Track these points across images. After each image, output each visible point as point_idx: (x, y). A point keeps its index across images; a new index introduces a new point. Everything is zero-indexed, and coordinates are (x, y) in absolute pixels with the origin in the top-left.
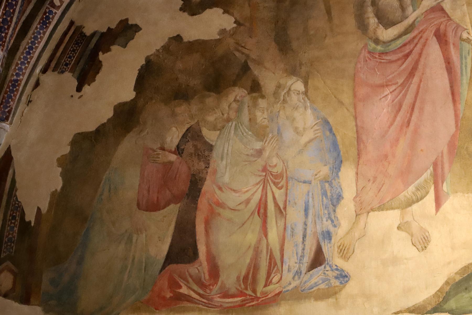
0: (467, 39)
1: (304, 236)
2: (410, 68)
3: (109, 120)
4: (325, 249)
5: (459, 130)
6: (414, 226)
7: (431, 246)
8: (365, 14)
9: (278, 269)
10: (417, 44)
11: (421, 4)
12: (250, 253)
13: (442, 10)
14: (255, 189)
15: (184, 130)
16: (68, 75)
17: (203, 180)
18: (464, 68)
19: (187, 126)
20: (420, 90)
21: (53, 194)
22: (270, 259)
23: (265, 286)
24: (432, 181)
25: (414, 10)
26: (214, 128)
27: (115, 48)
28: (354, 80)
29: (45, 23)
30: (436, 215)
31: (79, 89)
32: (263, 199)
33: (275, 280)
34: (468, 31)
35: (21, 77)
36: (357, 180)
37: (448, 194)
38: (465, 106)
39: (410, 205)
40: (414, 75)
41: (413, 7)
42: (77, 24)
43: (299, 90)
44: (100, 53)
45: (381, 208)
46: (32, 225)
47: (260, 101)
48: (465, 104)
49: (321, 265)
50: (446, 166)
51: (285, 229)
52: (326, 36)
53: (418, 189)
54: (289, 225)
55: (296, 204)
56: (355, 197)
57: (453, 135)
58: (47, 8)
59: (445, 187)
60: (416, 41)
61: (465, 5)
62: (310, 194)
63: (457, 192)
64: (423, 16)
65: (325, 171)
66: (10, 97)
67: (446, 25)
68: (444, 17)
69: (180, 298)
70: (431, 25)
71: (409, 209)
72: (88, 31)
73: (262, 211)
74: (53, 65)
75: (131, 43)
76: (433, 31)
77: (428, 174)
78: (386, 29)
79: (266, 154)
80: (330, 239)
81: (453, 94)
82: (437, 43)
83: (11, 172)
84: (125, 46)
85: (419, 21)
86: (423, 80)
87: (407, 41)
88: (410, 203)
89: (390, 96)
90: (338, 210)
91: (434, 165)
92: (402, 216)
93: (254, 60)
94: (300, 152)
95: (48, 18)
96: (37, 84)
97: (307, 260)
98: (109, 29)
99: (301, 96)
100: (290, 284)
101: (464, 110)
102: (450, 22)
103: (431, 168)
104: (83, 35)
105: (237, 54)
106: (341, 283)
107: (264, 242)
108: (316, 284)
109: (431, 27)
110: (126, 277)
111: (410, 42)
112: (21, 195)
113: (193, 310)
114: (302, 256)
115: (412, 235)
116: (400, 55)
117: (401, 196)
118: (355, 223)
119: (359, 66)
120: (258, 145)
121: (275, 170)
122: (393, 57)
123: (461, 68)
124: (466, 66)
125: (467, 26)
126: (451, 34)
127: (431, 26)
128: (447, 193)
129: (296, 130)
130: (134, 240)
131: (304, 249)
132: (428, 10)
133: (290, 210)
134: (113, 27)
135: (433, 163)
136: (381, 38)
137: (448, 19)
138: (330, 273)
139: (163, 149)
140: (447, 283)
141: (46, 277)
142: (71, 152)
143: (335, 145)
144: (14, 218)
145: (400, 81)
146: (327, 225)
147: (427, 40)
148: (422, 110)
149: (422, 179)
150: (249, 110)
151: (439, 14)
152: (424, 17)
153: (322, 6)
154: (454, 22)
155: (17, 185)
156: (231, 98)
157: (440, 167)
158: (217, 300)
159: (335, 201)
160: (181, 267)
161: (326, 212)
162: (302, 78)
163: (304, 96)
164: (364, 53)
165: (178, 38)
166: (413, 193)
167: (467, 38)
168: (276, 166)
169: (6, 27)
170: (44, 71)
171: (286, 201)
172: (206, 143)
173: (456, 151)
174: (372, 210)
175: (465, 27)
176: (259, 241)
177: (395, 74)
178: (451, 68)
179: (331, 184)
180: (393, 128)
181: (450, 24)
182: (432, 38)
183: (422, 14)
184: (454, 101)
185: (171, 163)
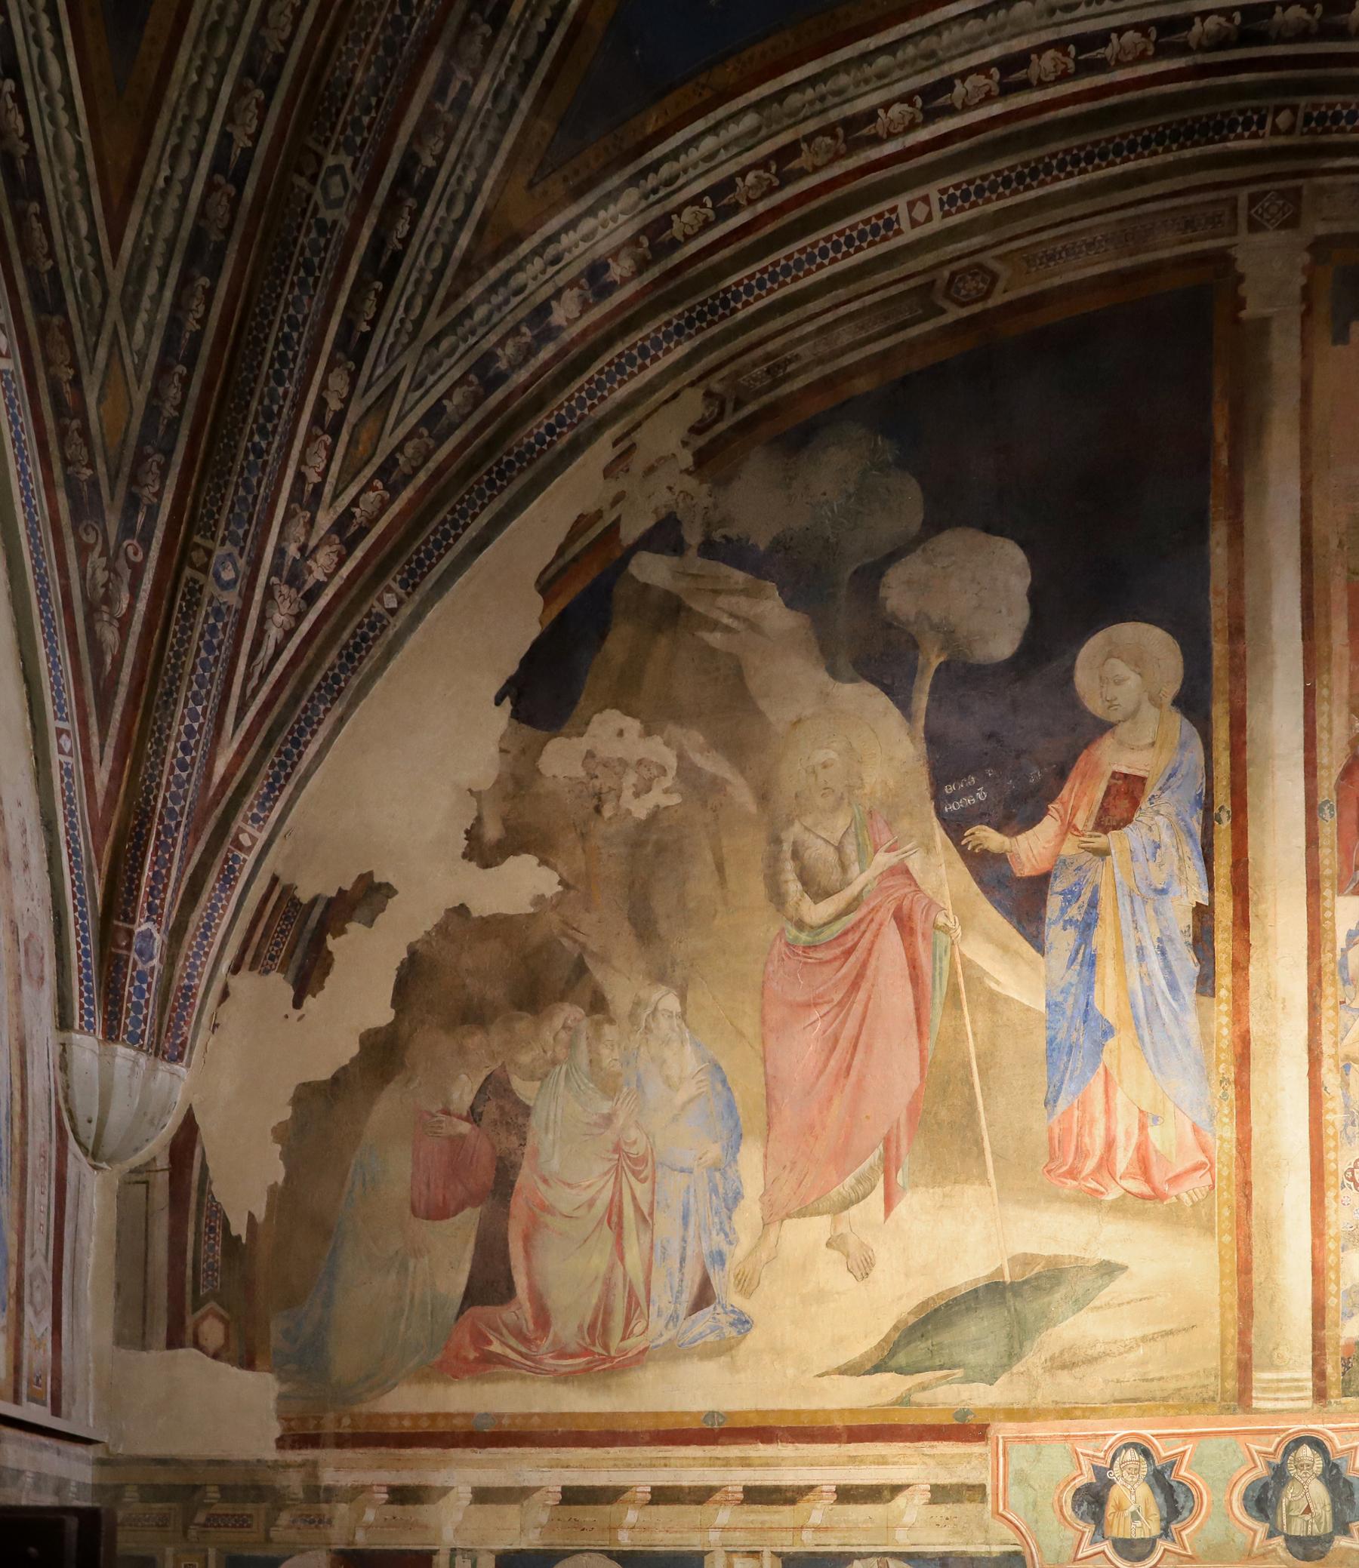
1: (683, 1260)
2: (854, 973)
3: (353, 1060)
4: (715, 1281)
6: (852, 1240)
7: (876, 1273)
9: (642, 1312)
12: (599, 1287)
13: (907, 872)
14: (602, 1183)
15: (481, 1080)
16: (276, 977)
17: (516, 1167)
19: (486, 1073)
21: (272, 1190)
22: (630, 1296)
23: (623, 1339)
25: (862, 871)
26: (532, 1078)
27: (353, 927)
28: (762, 994)
29: (228, 879)
31: (297, 1003)
32: (617, 1198)
33: (638, 1329)
35: (197, 981)
36: (765, 1168)
37: (904, 1189)
39: (847, 1208)
42: (284, 881)
44: (329, 937)
45: (802, 1213)
46: (244, 1241)
49: (708, 1305)
50: (904, 1142)
51: (652, 1248)
52: (716, 911)
53: (859, 1181)
54: (658, 1243)
55: (668, 1206)
56: (763, 1195)
58: (229, 850)
59: (900, 1178)
60: (863, 927)
62: (692, 1190)
65: (714, 1151)
66: (182, 1018)
69: (489, 1359)
71: (845, 1213)
72: (304, 895)
73: (614, 1219)
74: (249, 957)
75: (381, 918)
77: (874, 1158)
78: (816, 903)
79: (619, 1122)
80: (723, 1264)
83: (198, 1151)
84: (370, 923)
87: (849, 926)
88: (847, 1204)
89: (819, 1024)
90: (735, 1217)
92: (835, 1225)
93: (593, 955)
94: (675, 1119)
95: (231, 869)
96: (225, 994)
97: (688, 1297)
98: (341, 891)
99: (676, 1022)
100: (661, 1335)
103: (881, 1147)
104: (295, 903)
105: (566, 942)
106: (739, 1332)
107: (619, 1270)
108: (701, 1336)
110: (402, 1327)
111: (853, 928)
112: (221, 1190)
113: (512, 1378)
114: (680, 1292)
115: (848, 1256)
116: (838, 951)
117: (833, 1193)
118: (763, 1236)
119: (771, 968)
120: (606, 1107)
121: (633, 1150)
123: (934, 976)
129: (667, 1080)
130: (411, 1269)
131: (682, 1280)
133: (660, 1218)
134: (348, 887)
136: (807, 919)
138: (723, 1318)
139: (447, 1112)
140: (895, 1328)
141: (276, 1328)
142: (295, 1117)
143: (731, 1106)
144: (212, 1229)
145: (837, 997)
146: (718, 1241)
147: (881, 925)
148: (869, 1048)
149: (865, 1165)
150: (589, 1045)
151: (900, 880)
153: (709, 857)
155: (211, 1174)
156: (558, 1022)
157: (893, 1145)
158: (549, 1361)
159: (730, 1202)
160: (489, 1310)
161: (716, 1220)
162: (675, 987)
163: (680, 1021)
164: (780, 946)
165: (462, 910)
166: (852, 1188)
168: (635, 1142)
169: (161, 887)
170: (235, 969)
171: (652, 1203)
172: (518, 1102)
174: (789, 1216)
176: (612, 1268)
177: (830, 984)
178: (917, 976)
179: (724, 1174)
180: (823, 1079)
184: (920, 1034)
185: (462, 1137)
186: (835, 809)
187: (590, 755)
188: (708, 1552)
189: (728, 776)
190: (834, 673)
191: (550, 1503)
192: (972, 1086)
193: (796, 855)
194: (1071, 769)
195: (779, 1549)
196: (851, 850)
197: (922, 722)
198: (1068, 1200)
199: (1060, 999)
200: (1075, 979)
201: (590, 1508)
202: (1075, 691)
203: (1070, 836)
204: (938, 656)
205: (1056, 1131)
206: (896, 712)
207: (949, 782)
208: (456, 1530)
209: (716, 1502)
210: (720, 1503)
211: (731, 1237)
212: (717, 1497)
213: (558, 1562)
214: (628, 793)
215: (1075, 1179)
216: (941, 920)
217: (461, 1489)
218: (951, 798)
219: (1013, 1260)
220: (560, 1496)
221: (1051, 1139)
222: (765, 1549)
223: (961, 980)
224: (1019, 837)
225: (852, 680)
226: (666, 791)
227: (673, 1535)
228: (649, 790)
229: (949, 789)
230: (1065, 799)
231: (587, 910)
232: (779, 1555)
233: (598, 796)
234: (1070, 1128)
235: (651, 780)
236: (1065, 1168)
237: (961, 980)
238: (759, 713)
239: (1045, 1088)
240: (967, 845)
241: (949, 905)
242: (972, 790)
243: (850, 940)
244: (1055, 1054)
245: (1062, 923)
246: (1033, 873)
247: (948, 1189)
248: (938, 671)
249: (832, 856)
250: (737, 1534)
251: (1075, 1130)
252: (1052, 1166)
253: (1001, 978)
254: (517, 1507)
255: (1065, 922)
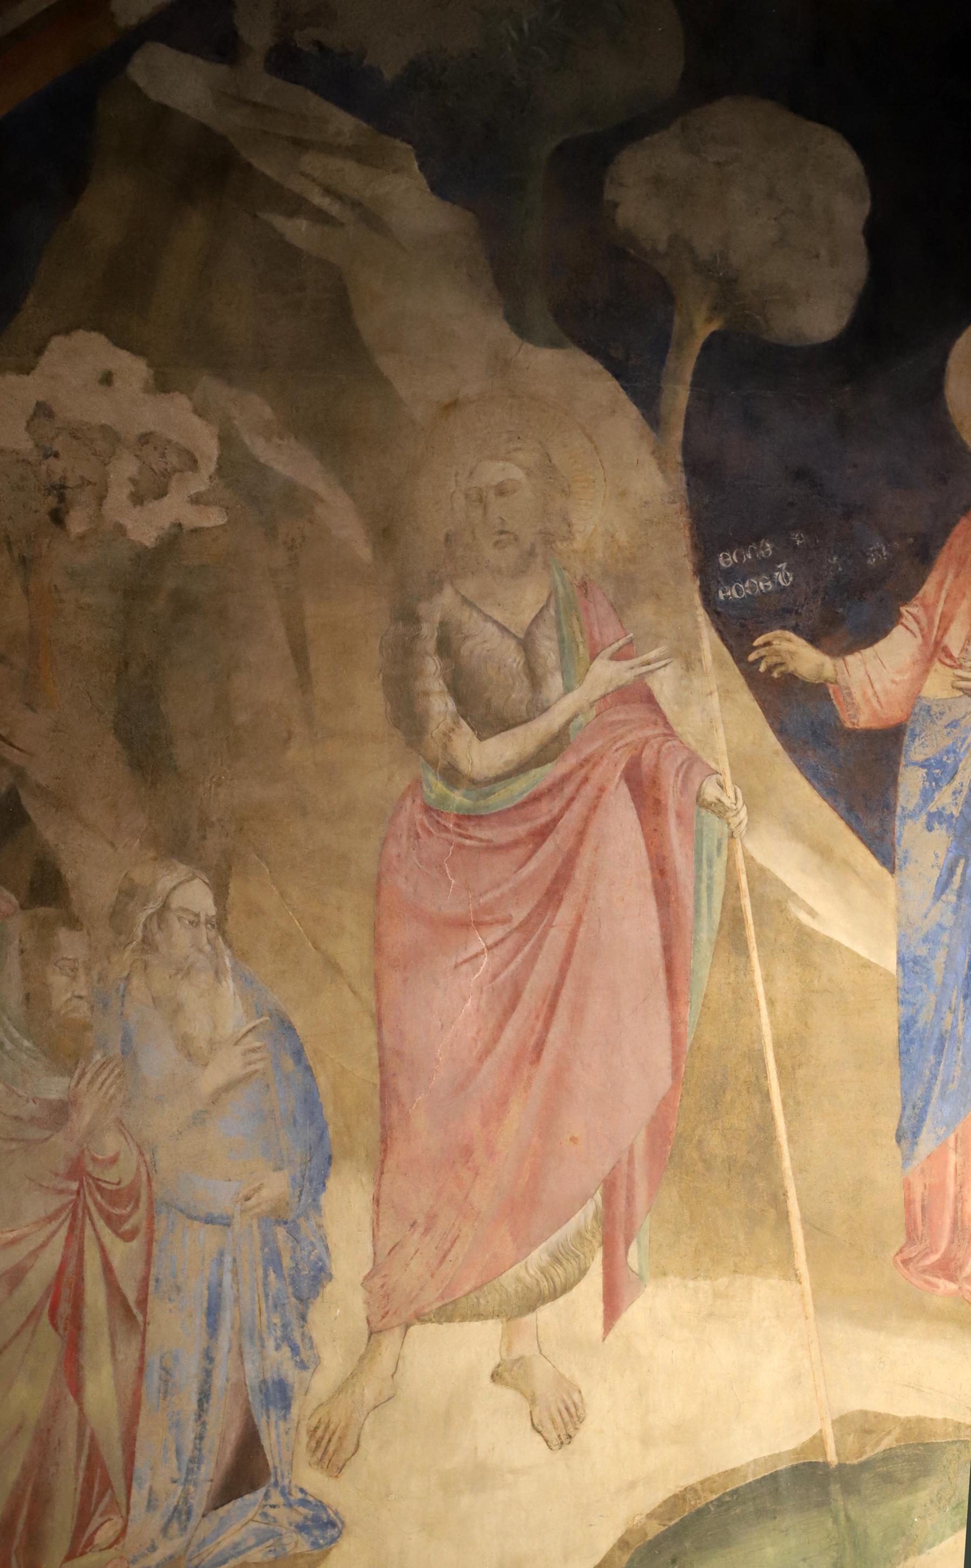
0: (715, 804)
1: (204, 1397)
2: (550, 875)
4: (270, 1439)
5: (683, 1085)
6: (541, 1373)
7: (586, 1435)
8: (416, 679)
9: (114, 1500)
10: (572, 799)
11: (587, 670)
12: (24, 1446)
13: (649, 699)
14: (42, 1236)
18: (704, 894)
20: (577, 949)
22: (90, 1468)
24: (599, 1238)
25: (568, 690)
28: (377, 895)
30: (604, 1340)
32: (71, 1268)
33: (105, 1534)
34: (721, 779)
36: (376, 1224)
37: (640, 1277)
38: (701, 1012)
39: (532, 1308)
40: (560, 900)
41: (563, 679)
43: (196, 910)
47: (63, 935)
48: (703, 1005)
49: (253, 1488)
51: (141, 1370)
52: (290, 735)
53: (556, 1259)
54: (153, 1360)
55: (178, 1289)
56: (369, 1277)
57: (664, 1098)
59: (634, 1258)
60: (568, 790)
61: (716, 695)
62: (228, 1259)
63: (665, 1274)
64: (594, 712)
67: (659, 752)
68: (656, 723)
70: (615, 742)
71: (530, 1318)
73: (65, 1309)
76: (622, 766)
78: (481, 738)
79: (83, 1118)
80: (287, 1407)
81: (669, 970)
82: (632, 805)
85: (581, 725)
86: (585, 918)
87: (543, 785)
89: (485, 960)
90: (315, 1315)
91: (605, 1187)
92: (508, 1341)
94: (199, 1120)
99: (204, 933)
100: (153, 1548)
101: (699, 1024)
102: (669, 744)
103: (598, 1197)
106: (315, 1544)
108: (237, 1550)
109: (617, 750)
114: (196, 1460)
115: (533, 1401)
116: (522, 830)
117: (508, 1280)
118: (366, 1359)
119: (393, 850)
121: (110, 1176)
122: (502, 834)
123: (697, 891)
124: (710, 888)
125: (718, 764)
126: (672, 781)
127: (614, 748)
128: (637, 1275)
129: (185, 1044)
131: (200, 1437)
132: (608, 694)
135: (603, 1181)
136: (465, 766)
137: (666, 731)
138: (282, 1515)
140: (623, 1544)
145: (519, 915)
147: (602, 790)
148: (578, 1011)
149: (570, 1228)
150: (25, 965)
151: (638, 712)
152: (597, 716)
153: (280, 635)
154: (681, 742)
157: (622, 1194)
159: (305, 1286)
161: (276, 1320)
162: (205, 869)
163: (213, 933)
164: (412, 812)
166: (543, 1271)
167: (716, 801)
168: (114, 1160)
171: (145, 1281)
173: (669, 1147)
174: (420, 1318)
175: (713, 765)
176: (54, 1409)
177: (506, 888)
178: (668, 890)
179: (294, 1232)
180: (490, 1063)
181: (670, 748)
182: (617, 787)
183: (591, 706)
184: (673, 994)
186: (520, 571)
187: (43, 411)
189: (320, 487)
190: (522, 328)
192: (767, 1097)
193: (445, 647)
194: (940, 547)
196: (548, 649)
197: (678, 435)
198: (938, 1316)
199: (922, 951)
200: (948, 919)
202: (946, 413)
203: (938, 665)
204: (709, 320)
205: (918, 1191)
206: (633, 411)
207: (726, 546)
211: (305, 1354)
214: (119, 495)
215: (952, 1278)
216: (711, 792)
218: (730, 576)
219: (842, 1423)
221: (908, 1203)
223: (746, 903)
224: (850, 658)
225: (554, 344)
226: (196, 500)
228: (162, 493)
229: (727, 560)
230: (930, 599)
231: (30, 706)
233: (60, 490)
234: (942, 1187)
235: (167, 475)
236: (934, 1258)
237: (746, 903)
238: (382, 382)
239: (898, 1109)
240: (758, 661)
241: (725, 766)
242: (766, 566)
243: (544, 812)
244: (914, 1048)
245: (924, 817)
246: (874, 725)
247: (722, 1282)
248: (707, 346)
249: (513, 659)
251: (951, 1190)
252: (912, 1252)
253: (819, 907)
255: (930, 815)
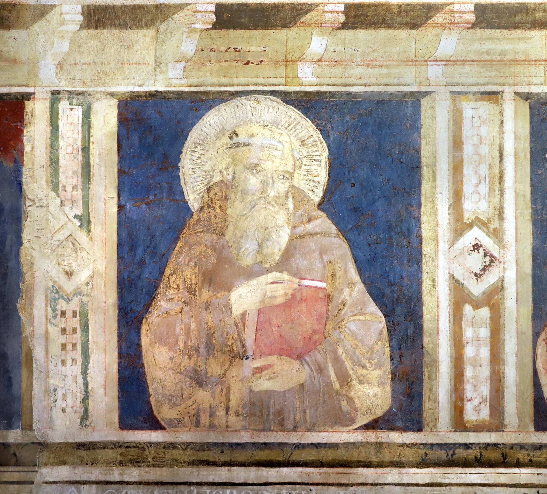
188: (427, 94)
191: (199, 26)
195: (525, 89)
201: (258, 33)
208: (60, 66)
209: (437, 25)
210: (443, 26)
212: (439, 18)
213: (211, 108)
217: (66, 8)
220: (213, 18)
222: (506, 88)
227: (376, 71)
232: (526, 97)
250: (467, 68)
254: (150, 33)
